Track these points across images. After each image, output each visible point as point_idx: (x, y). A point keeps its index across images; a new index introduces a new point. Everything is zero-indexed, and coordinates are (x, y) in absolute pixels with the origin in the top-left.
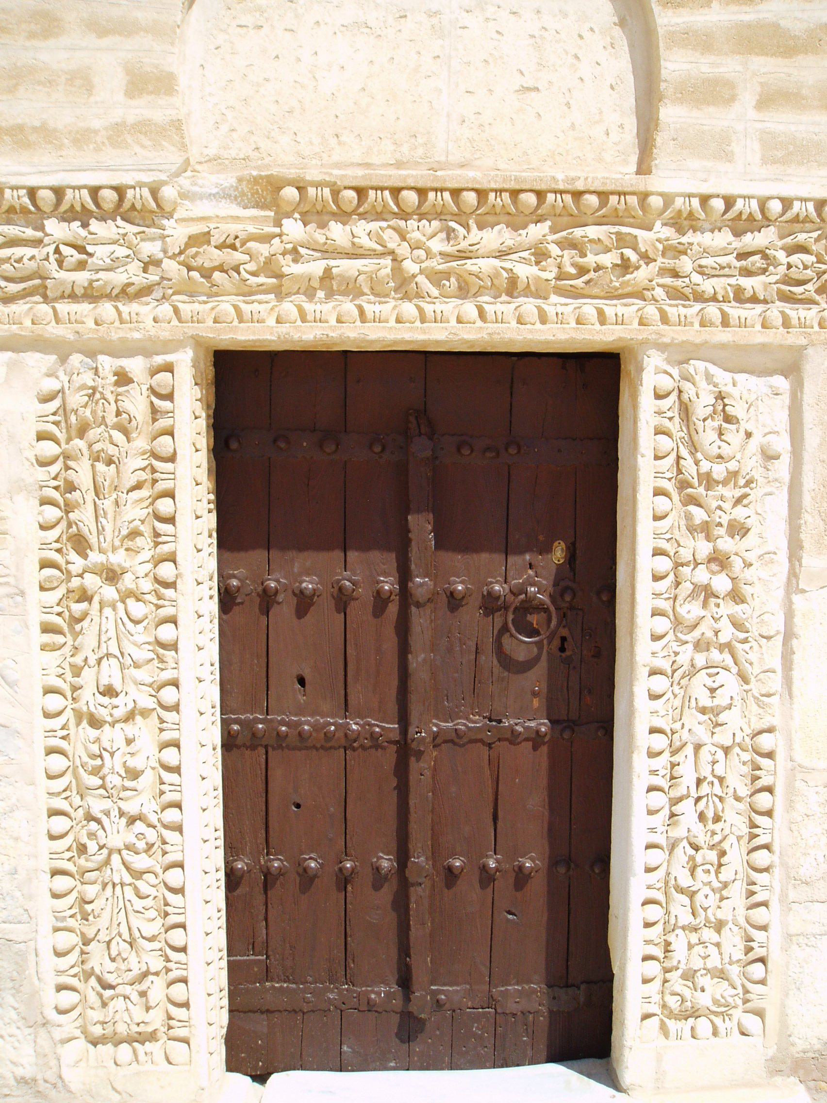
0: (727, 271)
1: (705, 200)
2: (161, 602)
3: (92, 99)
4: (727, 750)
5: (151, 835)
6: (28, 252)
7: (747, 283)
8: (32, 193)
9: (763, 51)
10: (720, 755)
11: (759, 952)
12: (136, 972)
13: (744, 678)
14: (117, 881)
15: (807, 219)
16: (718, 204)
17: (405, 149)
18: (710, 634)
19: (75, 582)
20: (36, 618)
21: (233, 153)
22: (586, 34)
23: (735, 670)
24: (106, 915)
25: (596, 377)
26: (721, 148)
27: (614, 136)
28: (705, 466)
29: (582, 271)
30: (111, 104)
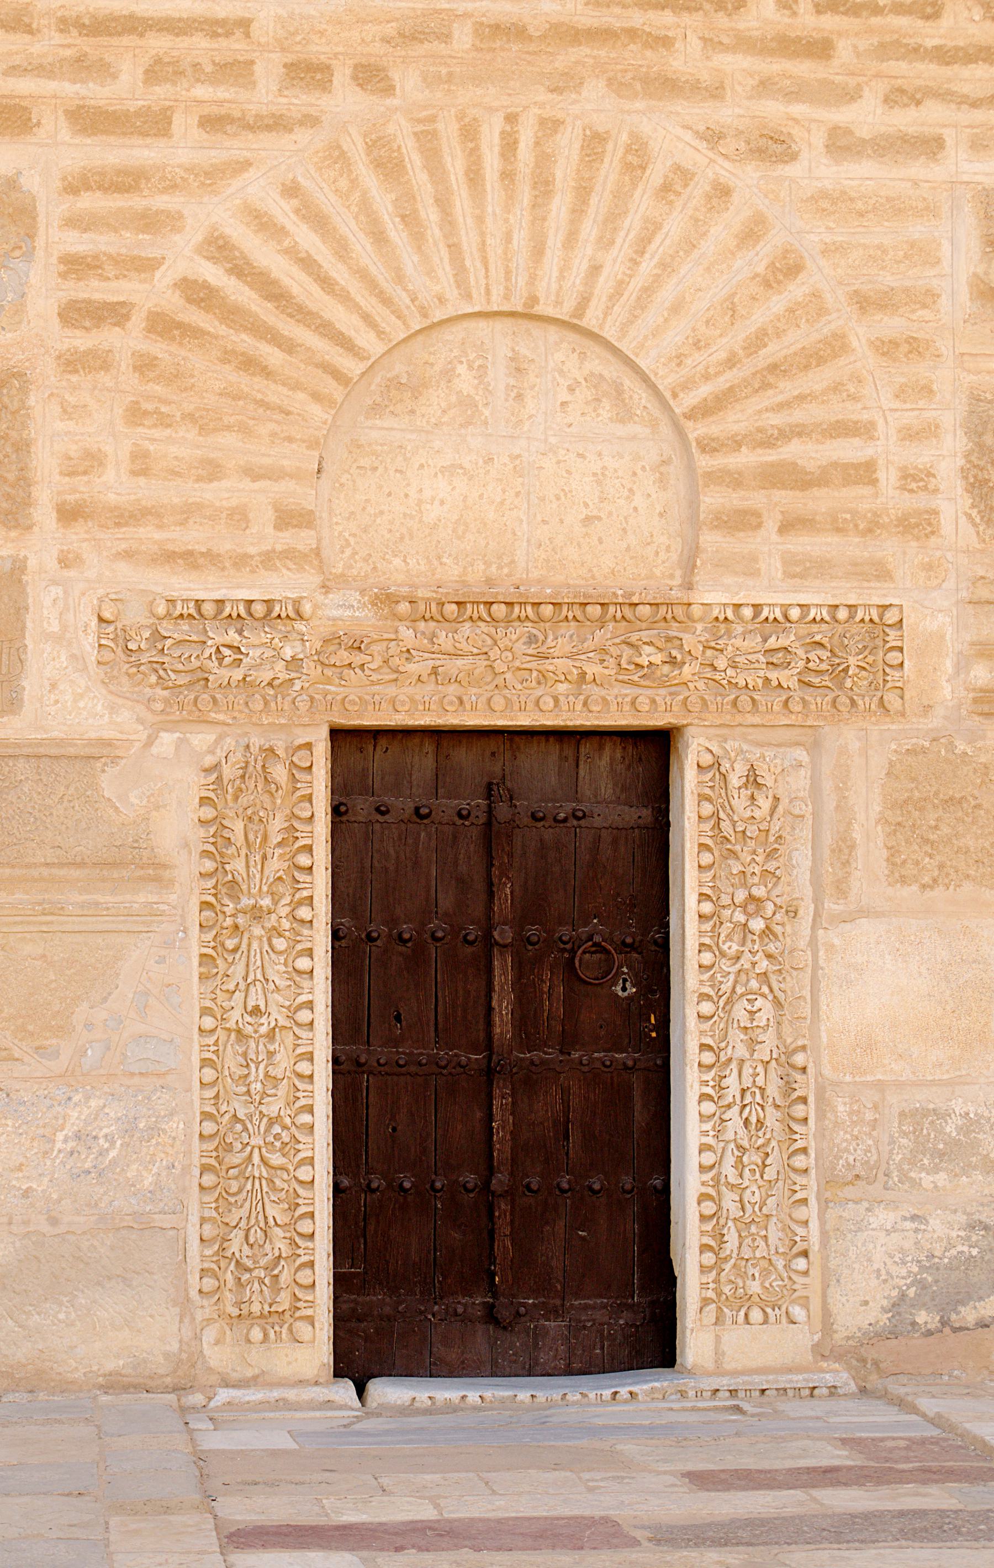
0: (756, 665)
1: (737, 607)
2: (298, 938)
3: (248, 532)
5: (285, 1137)
7: (773, 675)
10: (760, 1069)
11: (800, 1246)
12: (270, 1256)
13: (777, 1003)
14: (257, 1175)
16: (747, 612)
17: (494, 568)
18: (747, 966)
19: (229, 921)
20: (195, 951)
21: (355, 572)
22: (639, 472)
23: (770, 997)
24: (247, 1204)
27: (663, 555)
30: (263, 535)
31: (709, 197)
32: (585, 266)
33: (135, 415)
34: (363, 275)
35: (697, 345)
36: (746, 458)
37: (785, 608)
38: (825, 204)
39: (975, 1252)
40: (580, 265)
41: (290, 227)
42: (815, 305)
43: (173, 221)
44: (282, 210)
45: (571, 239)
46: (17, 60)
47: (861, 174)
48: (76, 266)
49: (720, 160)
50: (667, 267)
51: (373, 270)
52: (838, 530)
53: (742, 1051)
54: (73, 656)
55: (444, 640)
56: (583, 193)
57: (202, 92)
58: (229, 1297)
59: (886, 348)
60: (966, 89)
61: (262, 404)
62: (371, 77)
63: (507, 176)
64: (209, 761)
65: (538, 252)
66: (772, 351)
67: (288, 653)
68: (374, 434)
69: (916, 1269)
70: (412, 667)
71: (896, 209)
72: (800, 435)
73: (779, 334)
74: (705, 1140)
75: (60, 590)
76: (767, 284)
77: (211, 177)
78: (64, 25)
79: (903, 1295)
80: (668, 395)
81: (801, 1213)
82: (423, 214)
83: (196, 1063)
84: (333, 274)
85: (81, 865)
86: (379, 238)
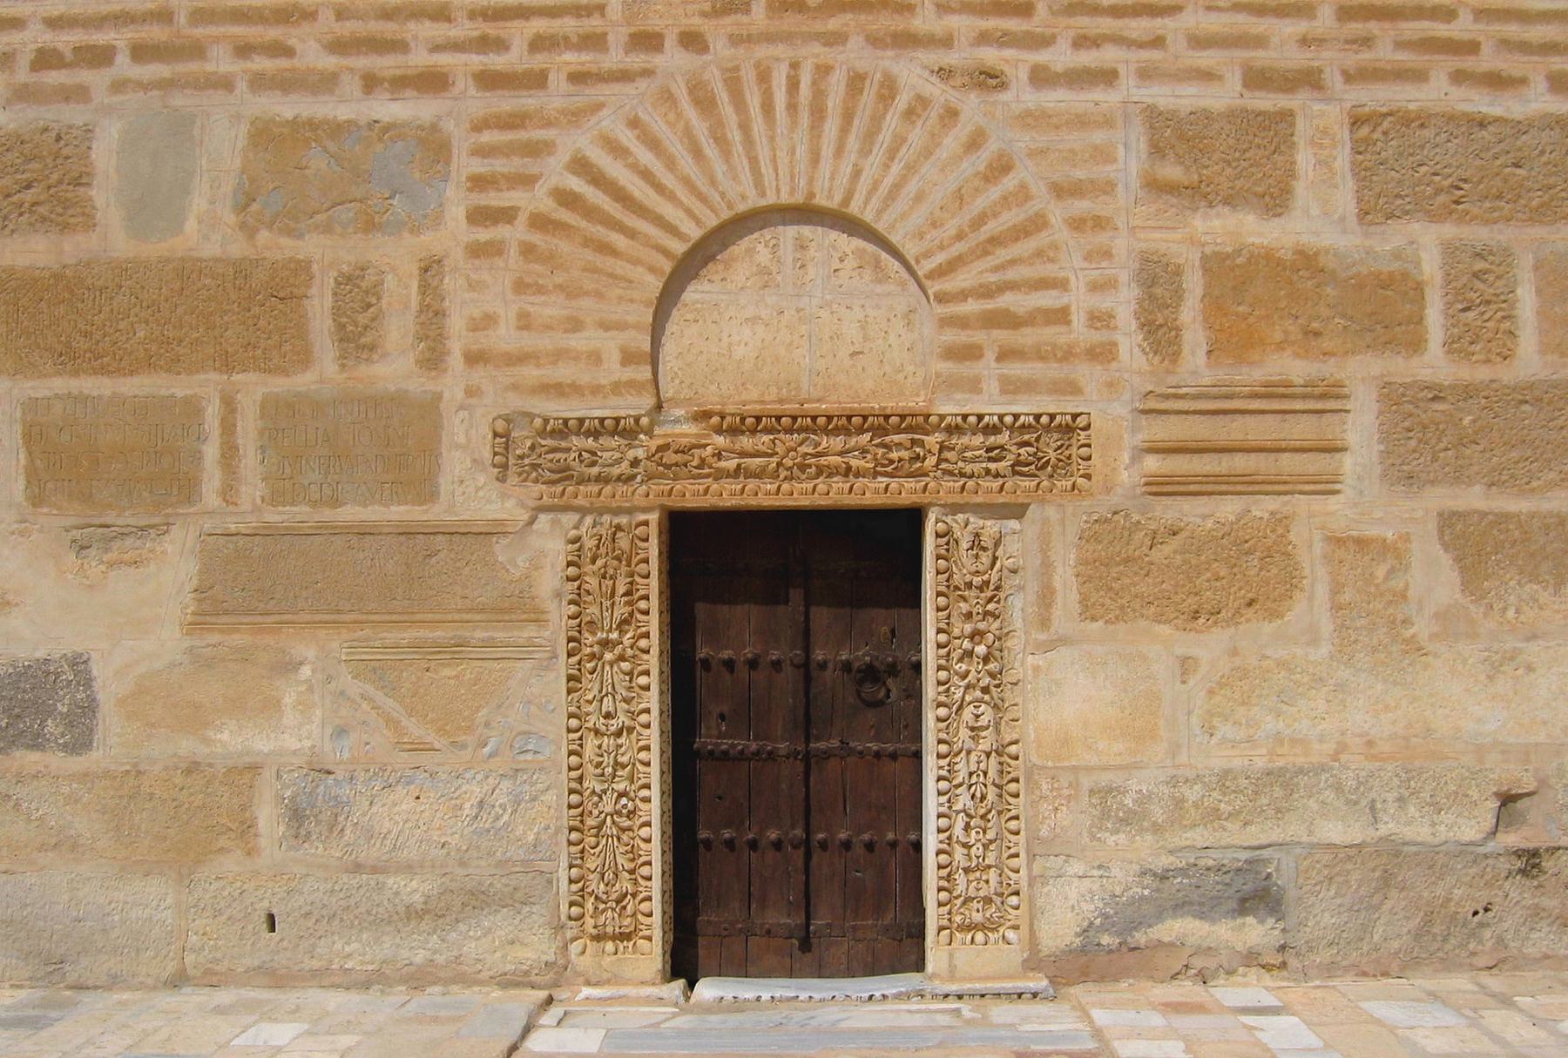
1: (965, 417)
4: (988, 755)
6: (562, 456)
7: (993, 466)
8: (566, 421)
9: (1000, 326)
10: (983, 757)
15: (1030, 426)
16: (972, 419)
19: (588, 650)
25: (905, 525)
26: (974, 386)
27: (910, 380)
28: (968, 578)
29: (892, 462)
30: (613, 370)
31: (941, 118)
32: (849, 170)
33: (520, 287)
34: (687, 182)
35: (934, 225)
36: (971, 307)
37: (1001, 417)
38: (1030, 120)
39: (1146, 892)
40: (846, 169)
41: (633, 148)
42: (1023, 194)
43: (546, 148)
44: (627, 138)
45: (839, 151)
46: (440, 41)
47: (1057, 99)
48: (479, 183)
49: (951, 91)
50: (911, 168)
51: (694, 178)
52: (1042, 358)
53: (969, 744)
54: (474, 461)
55: (746, 442)
56: (848, 117)
57: (569, 57)
58: (589, 922)
59: (1077, 224)
60: (1134, 35)
61: (612, 275)
62: (693, 41)
63: (792, 107)
64: (573, 533)
65: (815, 159)
66: (991, 228)
67: (631, 454)
68: (698, 296)
69: (1101, 905)
70: (723, 464)
71: (1082, 122)
72: (1012, 289)
73: (995, 215)
74: (942, 809)
76: (987, 179)
77: (575, 117)
78: (472, 15)
79: (1091, 923)
80: (913, 263)
81: (1014, 862)
82: (729, 136)
83: (564, 752)
84: (664, 181)
85: (482, 610)
86: (697, 153)
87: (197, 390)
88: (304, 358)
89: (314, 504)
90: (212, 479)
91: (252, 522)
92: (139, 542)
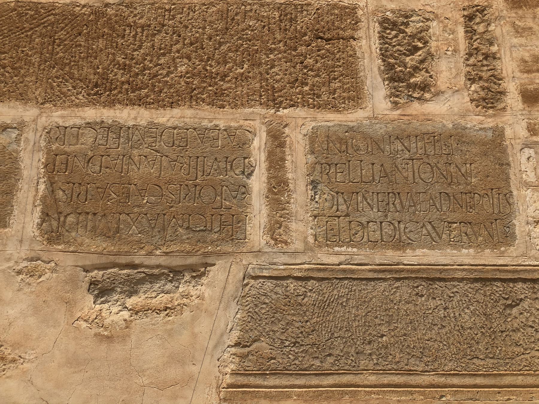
75: (532, 151)
87: (242, 122)
88: (355, 96)
89: (374, 244)
90: (258, 212)
91: (303, 263)
92: (169, 286)
